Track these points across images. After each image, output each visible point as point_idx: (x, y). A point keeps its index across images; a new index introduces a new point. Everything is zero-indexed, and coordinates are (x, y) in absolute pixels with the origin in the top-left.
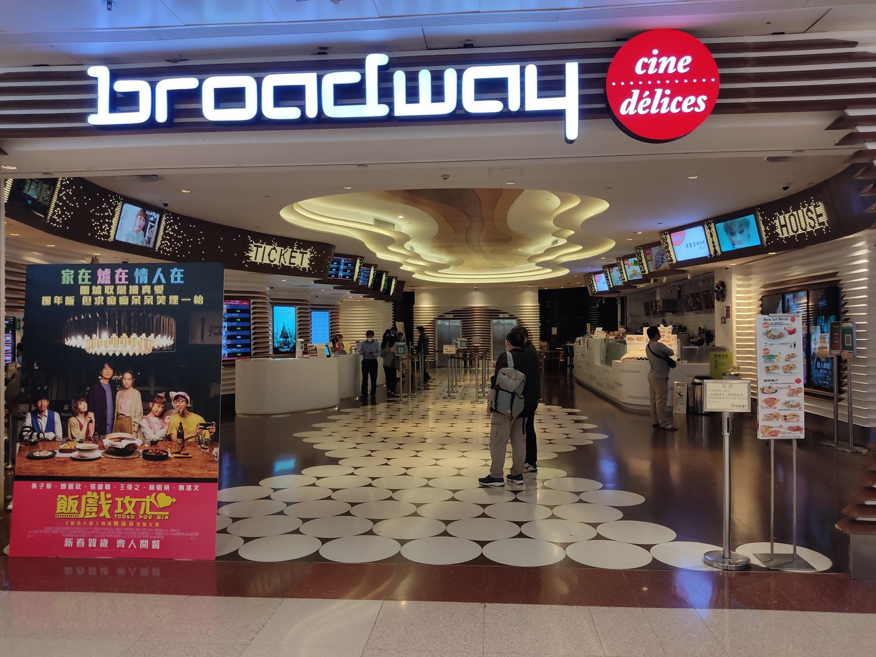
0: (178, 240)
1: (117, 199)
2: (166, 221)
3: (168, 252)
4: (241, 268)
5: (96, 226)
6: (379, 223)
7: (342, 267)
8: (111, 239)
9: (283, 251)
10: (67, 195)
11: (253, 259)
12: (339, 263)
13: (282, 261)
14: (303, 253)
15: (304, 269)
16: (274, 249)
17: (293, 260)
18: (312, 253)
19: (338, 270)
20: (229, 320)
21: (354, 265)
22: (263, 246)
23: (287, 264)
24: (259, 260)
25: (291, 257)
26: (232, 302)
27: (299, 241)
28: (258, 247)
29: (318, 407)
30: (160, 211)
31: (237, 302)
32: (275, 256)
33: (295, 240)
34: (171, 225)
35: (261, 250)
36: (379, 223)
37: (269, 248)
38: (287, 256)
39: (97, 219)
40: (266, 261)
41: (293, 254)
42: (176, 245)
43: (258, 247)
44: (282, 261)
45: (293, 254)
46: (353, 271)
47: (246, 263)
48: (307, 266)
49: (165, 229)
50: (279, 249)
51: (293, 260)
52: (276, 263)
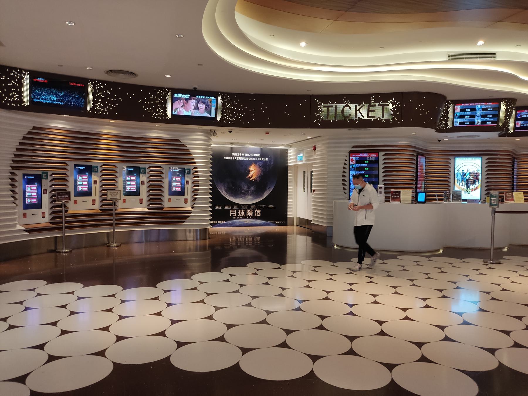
0: (241, 112)
1: (165, 91)
2: (223, 100)
3: (233, 121)
4: (315, 126)
5: (149, 110)
6: (454, 57)
7: (479, 113)
8: (169, 116)
9: (358, 107)
10: (106, 94)
11: (325, 118)
12: (473, 110)
13: (359, 115)
14: (383, 106)
15: (387, 120)
16: (347, 106)
17: (371, 114)
18: (393, 104)
19: (473, 116)
20: (357, 169)
21: (499, 109)
22: (334, 105)
23: (366, 118)
24: (332, 118)
25: (369, 111)
26: (361, 155)
27: (376, 95)
28: (328, 107)
29: (429, 249)
30: (215, 94)
31: (366, 155)
32: (347, 112)
33: (371, 95)
34: (229, 102)
35: (332, 110)
36: (454, 57)
37: (340, 107)
38: (364, 110)
39: (146, 106)
40: (340, 117)
41: (371, 108)
42: (239, 116)
43: (328, 107)
44: (359, 115)
45: (371, 108)
46: (498, 116)
47: (319, 122)
48: (391, 117)
49: (223, 105)
50: (353, 106)
51: (371, 114)
52: (352, 118)
